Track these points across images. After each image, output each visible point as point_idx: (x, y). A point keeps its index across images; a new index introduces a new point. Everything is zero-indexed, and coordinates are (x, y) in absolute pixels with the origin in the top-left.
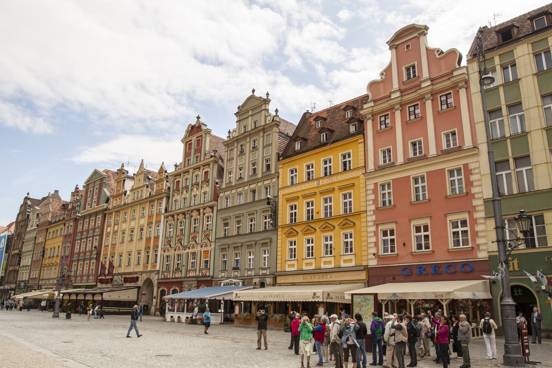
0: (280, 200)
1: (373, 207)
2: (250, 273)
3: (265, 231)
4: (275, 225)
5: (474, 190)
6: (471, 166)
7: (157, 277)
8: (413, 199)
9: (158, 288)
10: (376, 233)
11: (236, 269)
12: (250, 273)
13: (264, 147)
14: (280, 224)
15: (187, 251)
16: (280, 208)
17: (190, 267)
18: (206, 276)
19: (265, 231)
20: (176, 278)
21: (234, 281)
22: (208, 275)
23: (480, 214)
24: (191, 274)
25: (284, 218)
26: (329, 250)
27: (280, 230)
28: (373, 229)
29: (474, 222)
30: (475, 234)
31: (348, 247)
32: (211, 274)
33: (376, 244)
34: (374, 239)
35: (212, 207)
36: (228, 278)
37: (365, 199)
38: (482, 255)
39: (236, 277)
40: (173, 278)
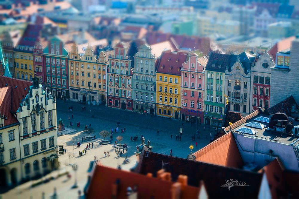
0: (157, 84)
1: (182, 95)
2: (147, 101)
3: (152, 91)
4: (155, 91)
5: (203, 98)
6: (203, 93)
7: (107, 94)
8: (191, 96)
9: (108, 98)
10: (183, 101)
11: (142, 99)
12: (147, 101)
13: (150, 65)
14: (157, 90)
15: (121, 89)
16: (157, 86)
17: (122, 94)
18: (130, 99)
19: (152, 91)
20: (116, 96)
21: (142, 102)
22: (131, 98)
23: (204, 103)
24: (123, 96)
25: (158, 89)
26: (171, 101)
27: (157, 92)
28: (182, 100)
29: (202, 104)
30: (202, 107)
31: (176, 102)
32: (132, 98)
33: (183, 103)
34: (182, 102)
35: (131, 77)
36: (139, 101)
37: (181, 91)
38: (203, 111)
39: (142, 102)
40: (114, 96)
